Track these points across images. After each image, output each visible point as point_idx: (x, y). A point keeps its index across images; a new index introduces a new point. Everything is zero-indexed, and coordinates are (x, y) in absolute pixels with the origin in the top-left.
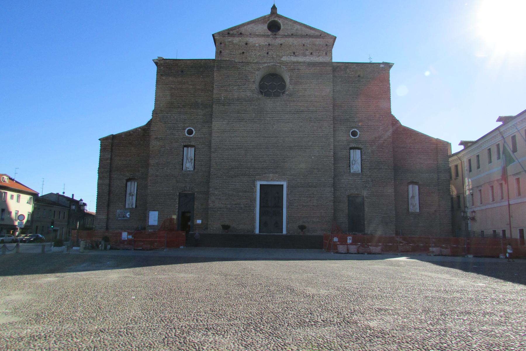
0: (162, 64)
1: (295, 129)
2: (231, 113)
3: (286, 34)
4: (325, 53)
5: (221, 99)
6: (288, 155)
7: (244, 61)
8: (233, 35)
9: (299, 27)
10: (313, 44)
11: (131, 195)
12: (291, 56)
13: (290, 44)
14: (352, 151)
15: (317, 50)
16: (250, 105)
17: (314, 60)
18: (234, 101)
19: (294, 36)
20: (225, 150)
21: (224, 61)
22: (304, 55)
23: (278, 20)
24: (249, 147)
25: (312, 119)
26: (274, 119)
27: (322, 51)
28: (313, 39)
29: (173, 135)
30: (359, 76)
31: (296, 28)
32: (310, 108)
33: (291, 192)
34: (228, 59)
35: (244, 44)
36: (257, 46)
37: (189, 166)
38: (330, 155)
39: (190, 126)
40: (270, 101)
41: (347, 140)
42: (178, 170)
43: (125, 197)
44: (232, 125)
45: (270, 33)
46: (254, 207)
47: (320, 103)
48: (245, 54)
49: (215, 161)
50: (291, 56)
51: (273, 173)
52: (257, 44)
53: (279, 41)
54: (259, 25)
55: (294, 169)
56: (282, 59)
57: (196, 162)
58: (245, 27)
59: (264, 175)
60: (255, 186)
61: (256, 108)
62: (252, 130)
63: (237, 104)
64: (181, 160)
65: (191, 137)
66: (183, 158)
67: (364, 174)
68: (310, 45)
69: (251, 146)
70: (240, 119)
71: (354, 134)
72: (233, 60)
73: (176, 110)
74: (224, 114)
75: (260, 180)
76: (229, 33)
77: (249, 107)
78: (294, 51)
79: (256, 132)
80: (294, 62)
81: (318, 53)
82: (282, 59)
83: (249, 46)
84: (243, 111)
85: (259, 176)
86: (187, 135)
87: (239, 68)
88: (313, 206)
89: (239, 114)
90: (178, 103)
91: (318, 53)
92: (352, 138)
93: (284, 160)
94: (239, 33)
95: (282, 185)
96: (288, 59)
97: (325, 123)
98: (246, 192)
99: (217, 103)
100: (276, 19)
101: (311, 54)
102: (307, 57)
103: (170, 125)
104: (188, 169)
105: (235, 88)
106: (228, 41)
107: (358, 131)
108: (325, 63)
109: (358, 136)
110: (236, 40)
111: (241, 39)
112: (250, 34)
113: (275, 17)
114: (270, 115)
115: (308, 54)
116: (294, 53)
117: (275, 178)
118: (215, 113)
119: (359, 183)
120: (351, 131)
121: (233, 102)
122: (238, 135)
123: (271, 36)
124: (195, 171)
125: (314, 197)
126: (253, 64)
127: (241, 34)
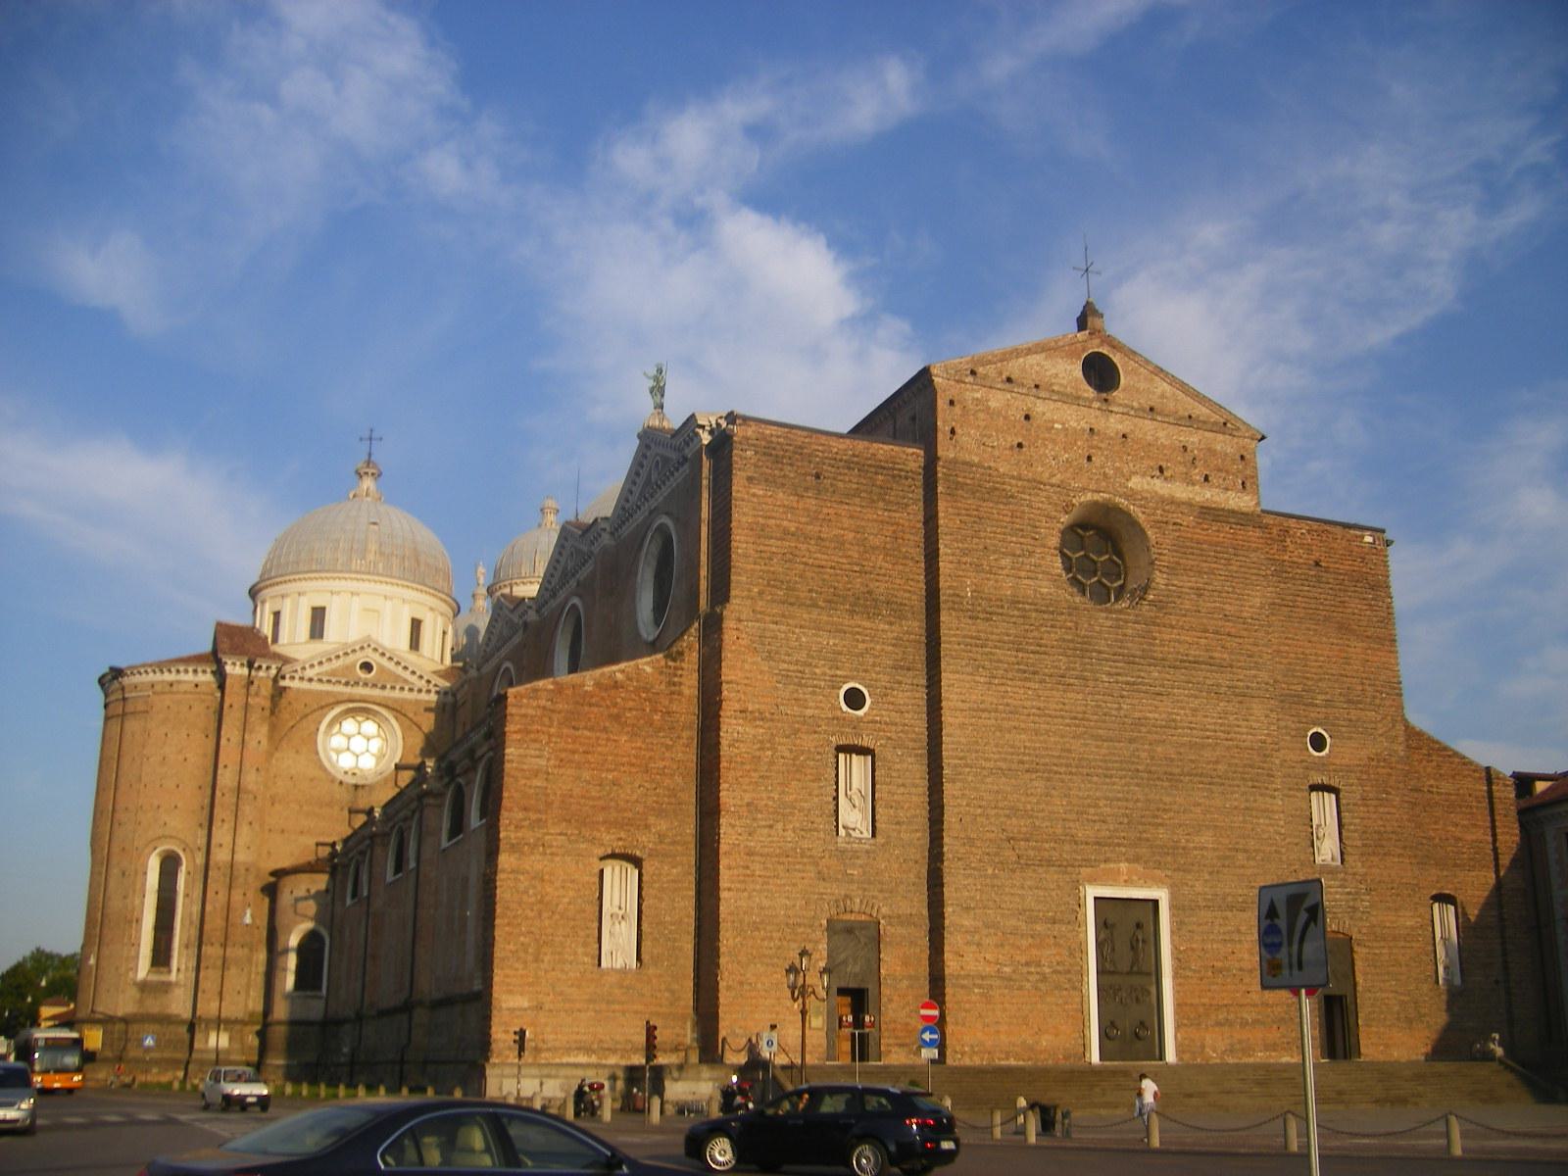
0: (748, 439)
1: (1178, 718)
2: (996, 647)
3: (1135, 404)
5: (962, 594)
6: (1165, 804)
12: (1152, 477)
13: (1149, 438)
14: (1314, 794)
15: (1220, 470)
16: (1052, 626)
17: (1216, 498)
18: (1002, 607)
19: (1159, 414)
20: (985, 773)
21: (965, 463)
23: (1111, 356)
24: (1055, 768)
25: (1222, 690)
26: (1120, 678)
28: (1206, 433)
29: (799, 706)
31: (1159, 391)
32: (1216, 655)
33: (1182, 923)
34: (976, 459)
35: (1020, 416)
37: (854, 818)
38: (1275, 808)
39: (853, 678)
40: (1107, 618)
41: (1302, 761)
44: (1003, 688)
45: (1090, 392)
47: (1241, 641)
49: (956, 810)
50: (1152, 477)
51: (1128, 860)
52: (1057, 422)
53: (1114, 424)
55: (1184, 848)
56: (1130, 485)
57: (879, 809)
58: (1021, 360)
59: (1102, 866)
60: (1080, 904)
61: (1070, 637)
62: (1061, 710)
63: (1014, 620)
64: (831, 799)
65: (860, 719)
66: (837, 790)
67: (1350, 871)
69: (1061, 765)
71: (1318, 742)
72: (992, 464)
74: (974, 649)
75: (1093, 880)
76: (973, 373)
77: (1049, 632)
78: (1161, 463)
79: (1075, 718)
80: (1163, 500)
81: (1224, 479)
82: (1130, 485)
84: (1031, 644)
85: (1089, 870)
87: (1012, 497)
88: (1241, 969)
89: (1020, 655)
90: (810, 591)
91: (1224, 479)
92: (1315, 757)
93: (1157, 817)
94: (1004, 377)
95: (1156, 902)
96: (1146, 487)
97: (1254, 706)
99: (953, 609)
100: (1105, 350)
101: (1206, 479)
103: (785, 666)
105: (1003, 562)
106: (973, 399)
108: (1242, 514)
109: (1327, 750)
110: (997, 400)
111: (1009, 396)
114: (1111, 667)
116: (1161, 470)
117: (1135, 878)
118: (950, 643)
119: (1338, 896)
120: (1309, 734)
121: (1000, 611)
122: (1023, 725)
123: (1096, 405)
124: (880, 839)
125: (1240, 941)
127: (1009, 380)
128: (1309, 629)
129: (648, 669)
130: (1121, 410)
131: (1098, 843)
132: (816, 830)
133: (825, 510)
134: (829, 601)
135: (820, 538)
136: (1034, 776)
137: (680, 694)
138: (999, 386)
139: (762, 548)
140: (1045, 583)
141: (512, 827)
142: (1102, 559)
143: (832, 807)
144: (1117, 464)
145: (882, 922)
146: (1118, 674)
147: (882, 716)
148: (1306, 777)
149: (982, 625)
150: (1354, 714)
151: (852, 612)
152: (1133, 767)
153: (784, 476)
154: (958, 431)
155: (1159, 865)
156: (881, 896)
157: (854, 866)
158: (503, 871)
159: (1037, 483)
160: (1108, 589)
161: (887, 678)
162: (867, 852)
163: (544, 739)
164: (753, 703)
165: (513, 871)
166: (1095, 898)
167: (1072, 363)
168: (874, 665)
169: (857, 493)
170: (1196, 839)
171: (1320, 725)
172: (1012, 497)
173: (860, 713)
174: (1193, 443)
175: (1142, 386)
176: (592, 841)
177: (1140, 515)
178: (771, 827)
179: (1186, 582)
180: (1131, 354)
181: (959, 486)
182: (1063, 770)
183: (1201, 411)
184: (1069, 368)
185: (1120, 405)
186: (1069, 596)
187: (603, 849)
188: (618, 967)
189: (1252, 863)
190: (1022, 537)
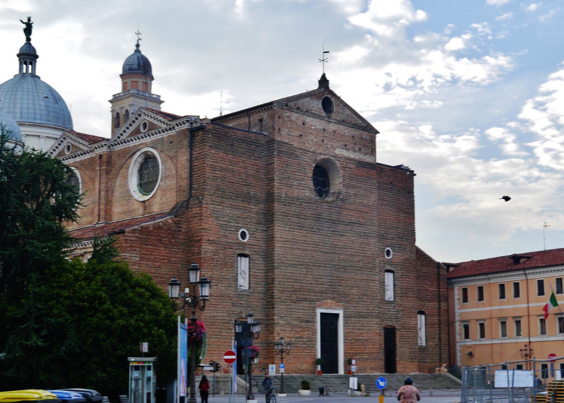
8: (290, 109)
9: (348, 112)
14: (386, 274)
18: (293, 201)
21: (283, 143)
22: (355, 151)
34: (287, 141)
35: (301, 124)
37: (243, 282)
40: (326, 206)
41: (383, 261)
45: (324, 114)
46: (315, 341)
48: (302, 137)
51: (330, 299)
53: (332, 127)
58: (302, 100)
59: (323, 301)
65: (245, 243)
68: (358, 138)
70: (300, 226)
72: (292, 143)
75: (320, 306)
76: (287, 105)
78: (346, 143)
84: (302, 215)
87: (298, 157)
88: (364, 340)
95: (337, 315)
96: (341, 153)
101: (360, 150)
112: (307, 111)
113: (328, 94)
116: (346, 145)
118: (277, 215)
120: (386, 250)
123: (326, 119)
126: (311, 154)
127: (298, 108)
129: (170, 221)
131: (322, 293)
136: (302, 267)
137: (181, 231)
138: (295, 111)
139: (214, 175)
140: (307, 192)
142: (322, 179)
144: (332, 144)
146: (329, 228)
148: (384, 267)
149: (288, 208)
151: (243, 201)
153: (221, 145)
154: (281, 129)
160: (322, 191)
161: (253, 227)
167: (319, 101)
170: (352, 291)
171: (389, 247)
172: (298, 157)
174: (356, 135)
175: (341, 111)
177: (338, 164)
178: (217, 285)
180: (338, 98)
181: (281, 152)
182: (311, 264)
185: (333, 119)
186: (313, 196)
189: (368, 300)
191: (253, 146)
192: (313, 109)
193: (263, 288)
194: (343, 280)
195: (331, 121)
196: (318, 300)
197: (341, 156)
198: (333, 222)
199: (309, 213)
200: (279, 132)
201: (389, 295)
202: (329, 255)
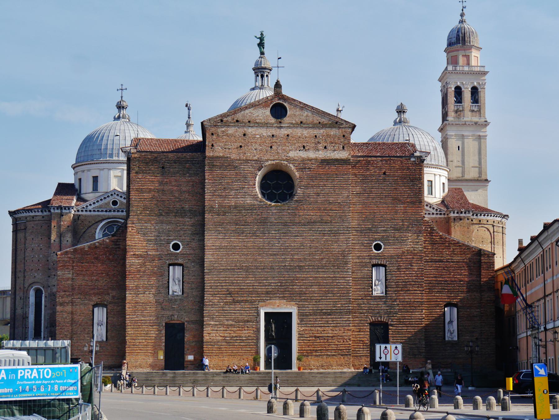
3: (294, 122)
4: (342, 146)
7: (242, 157)
10: (327, 135)
11: (100, 324)
12: (300, 151)
13: (299, 134)
15: (332, 143)
16: (251, 215)
17: (328, 155)
19: (304, 124)
22: (318, 150)
23: (284, 103)
27: (338, 144)
30: (384, 173)
34: (221, 155)
36: (258, 138)
39: (175, 239)
40: (275, 210)
42: (163, 295)
43: (92, 327)
45: (272, 120)
50: (300, 151)
53: (284, 132)
54: (260, 109)
57: (185, 285)
58: (243, 112)
60: (258, 315)
66: (169, 279)
71: (378, 247)
72: (229, 156)
73: (158, 219)
76: (222, 121)
80: (303, 160)
81: (334, 147)
83: (247, 137)
86: (172, 250)
90: (159, 210)
91: (334, 147)
95: (290, 314)
96: (296, 155)
98: (248, 321)
101: (325, 147)
102: (320, 152)
104: (175, 294)
107: (382, 244)
110: (231, 131)
115: (321, 148)
116: (304, 147)
120: (374, 244)
124: (185, 295)
127: (237, 121)
128: (377, 202)
130: (286, 125)
132: (161, 293)
133: (165, 180)
134: (167, 213)
135: (163, 190)
141: (60, 298)
143: (167, 285)
145: (186, 323)
147: (187, 252)
150: (397, 235)
152: (283, 264)
155: (292, 300)
156: (185, 314)
157: (175, 305)
158: (58, 312)
159: (247, 161)
162: (180, 299)
163: (71, 268)
164: (138, 252)
165: (61, 312)
166: (265, 313)
168: (184, 234)
169: (178, 172)
171: (379, 240)
173: (178, 251)
176: (89, 300)
177: (292, 167)
179: (310, 191)
183: (324, 120)
184: (264, 111)
187: (93, 302)
188: (100, 340)
190: (240, 182)
191: (188, 165)
192: (257, 118)
193: (200, 292)
194: (297, 280)
195: (282, 125)
196: (264, 301)
197: (297, 158)
198: (285, 224)
199: (249, 220)
200: (211, 148)
201: (378, 290)
202: (278, 257)
